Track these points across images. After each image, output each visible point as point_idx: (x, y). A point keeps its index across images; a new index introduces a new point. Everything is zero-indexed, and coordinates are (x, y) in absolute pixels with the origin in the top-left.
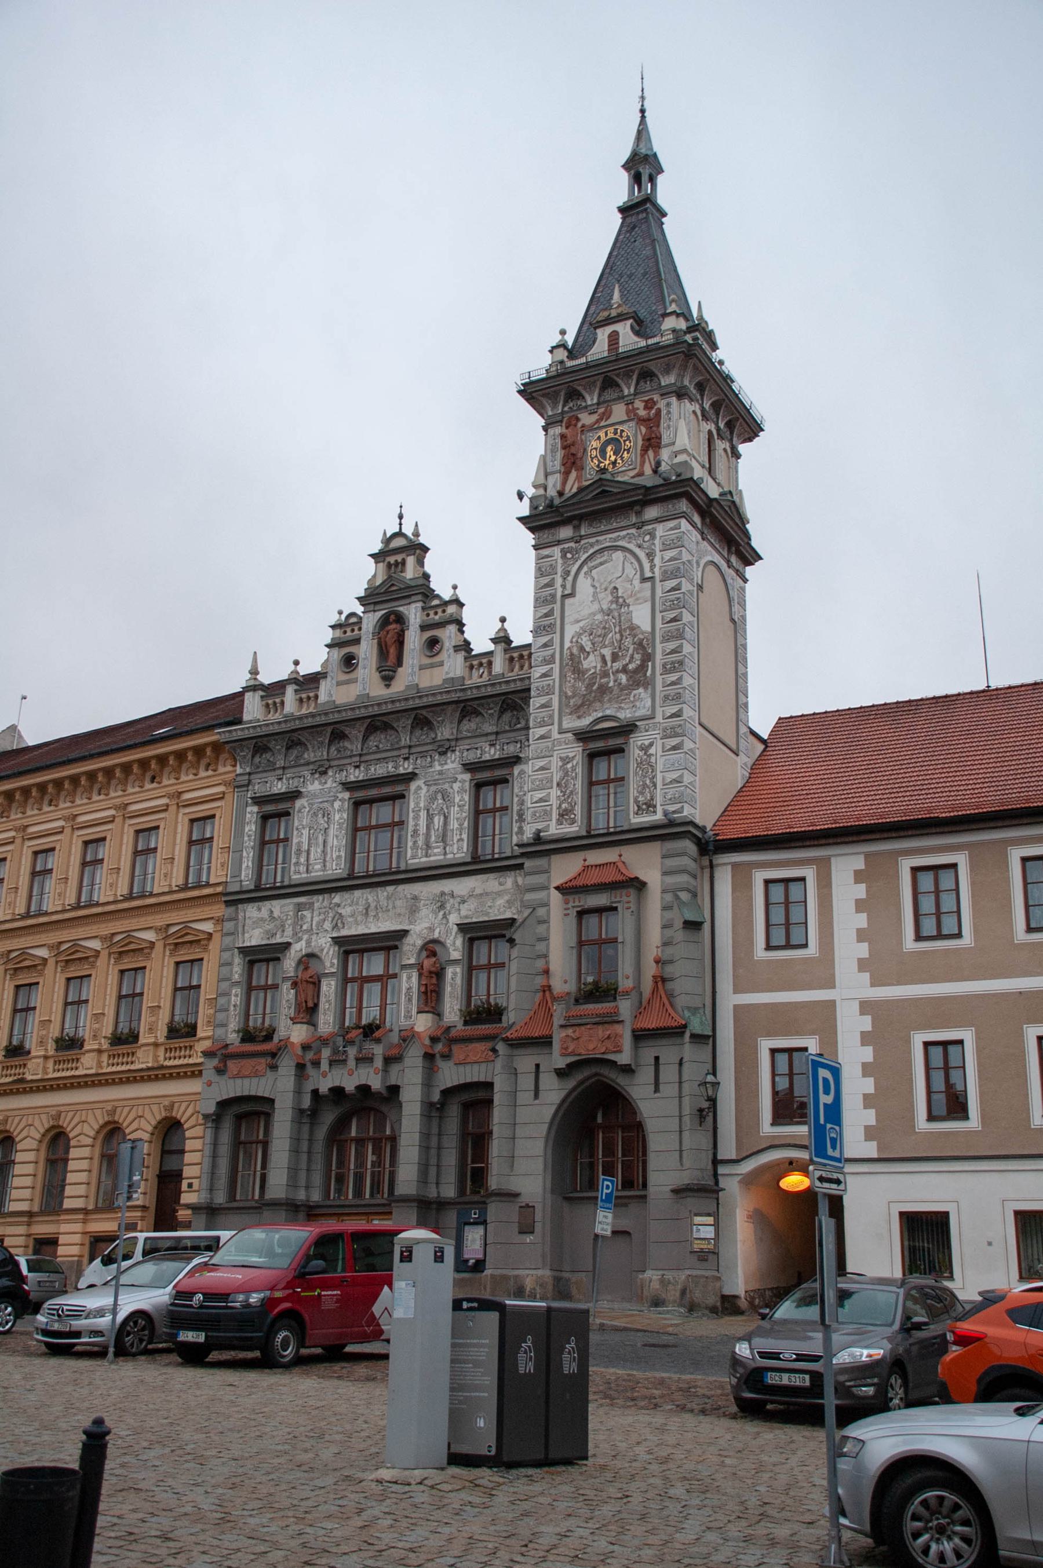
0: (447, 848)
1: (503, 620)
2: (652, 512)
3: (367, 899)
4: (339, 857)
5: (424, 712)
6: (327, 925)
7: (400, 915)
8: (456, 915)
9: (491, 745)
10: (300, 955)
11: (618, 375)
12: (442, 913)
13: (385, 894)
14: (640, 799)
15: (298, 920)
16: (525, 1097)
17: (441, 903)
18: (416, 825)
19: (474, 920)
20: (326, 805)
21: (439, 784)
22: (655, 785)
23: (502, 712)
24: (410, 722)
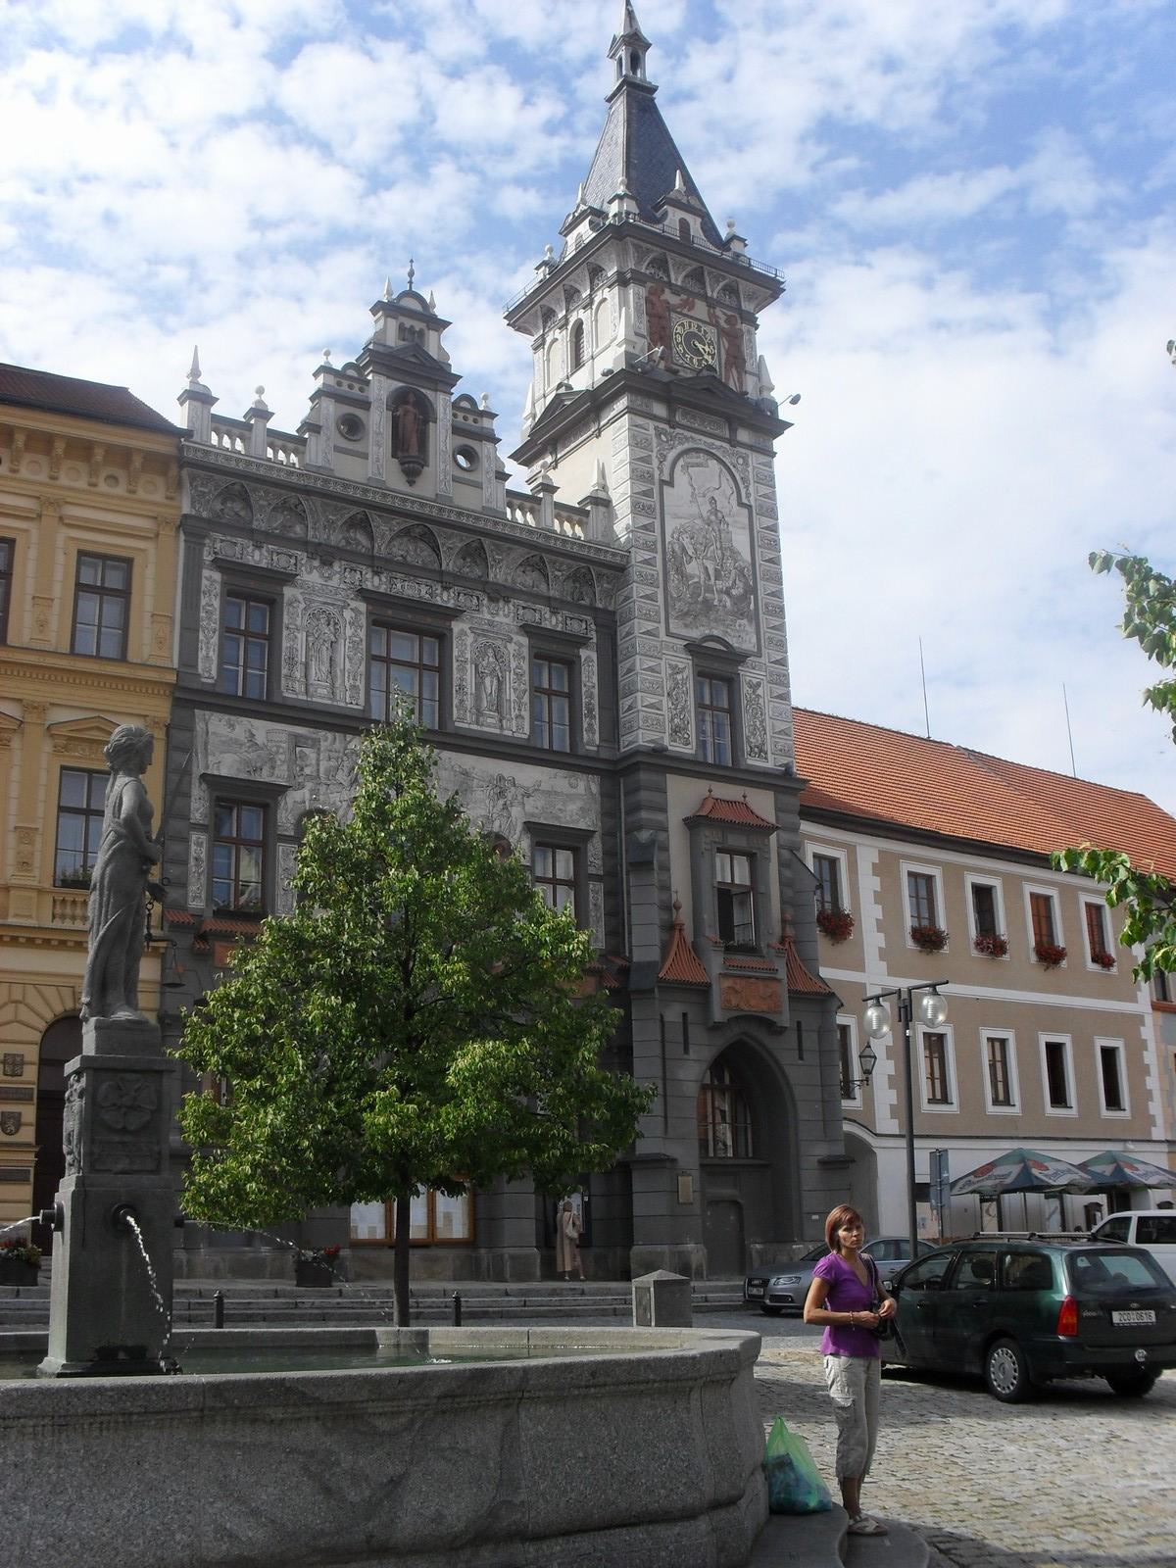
4: (354, 687)
5: (487, 543)
6: (341, 776)
10: (300, 809)
11: (710, 273)
12: (501, 802)
17: (500, 788)
24: (460, 545)
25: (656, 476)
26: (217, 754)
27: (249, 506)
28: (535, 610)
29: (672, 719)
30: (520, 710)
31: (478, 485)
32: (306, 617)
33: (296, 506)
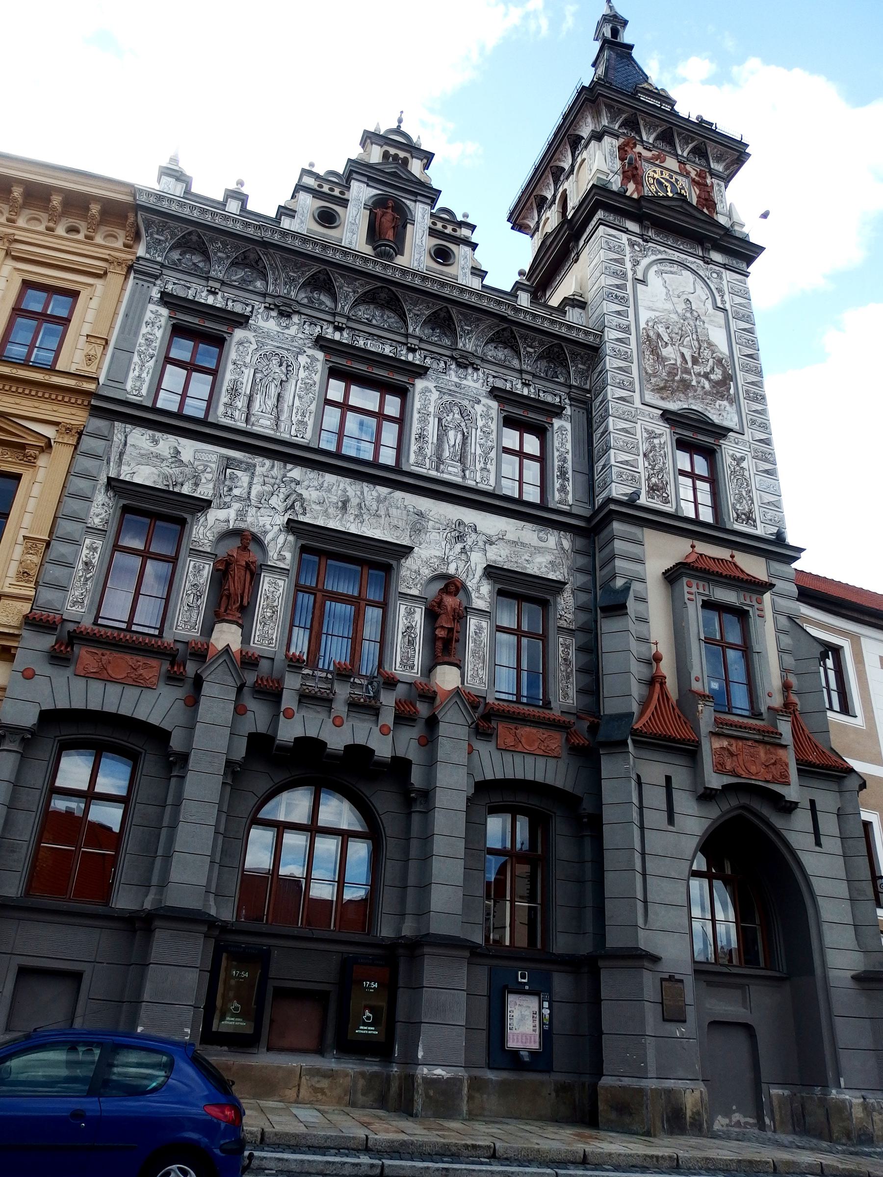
0: (467, 472)
2: (716, 256)
3: (345, 491)
8: (480, 554)
10: (223, 527)
11: (679, 134)
12: (459, 546)
13: (375, 494)
14: (738, 507)
16: (656, 818)
17: (459, 533)
20: (285, 353)
21: (456, 397)
22: (752, 500)
25: (630, 274)
26: (133, 465)
27: (207, 258)
28: (506, 380)
29: (649, 479)
33: (257, 262)
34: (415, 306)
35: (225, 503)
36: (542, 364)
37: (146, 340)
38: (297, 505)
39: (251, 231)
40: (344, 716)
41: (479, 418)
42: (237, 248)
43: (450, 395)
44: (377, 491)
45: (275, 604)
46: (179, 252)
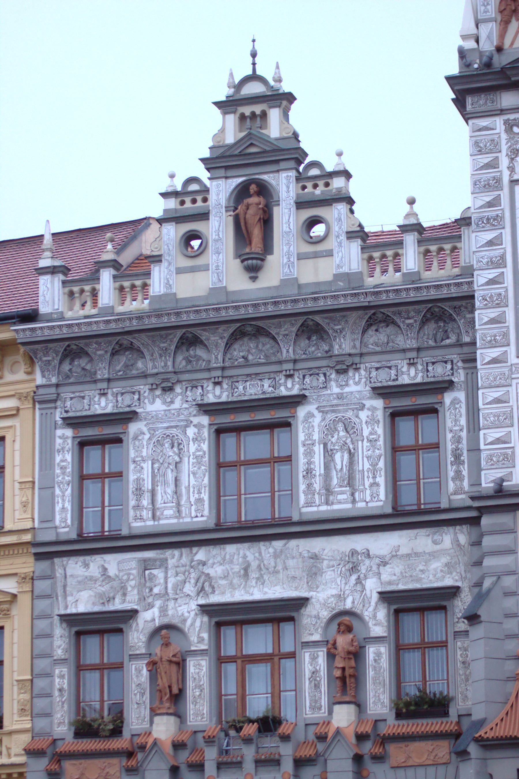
0: (357, 495)
1: (412, 202)
3: (245, 557)
4: (200, 501)
5: (317, 318)
6: (189, 588)
7: (294, 578)
9: (410, 364)
10: (151, 627)
12: (354, 577)
13: (271, 550)
15: (145, 581)
17: (352, 564)
18: (309, 463)
19: (401, 587)
20: (174, 431)
21: (339, 411)
23: (424, 322)
24: (294, 329)
26: (75, 593)
27: (91, 360)
28: (390, 368)
30: (374, 477)
31: (330, 254)
32: (151, 446)
34: (280, 327)
35: (149, 604)
36: (430, 328)
37: (61, 468)
38: (207, 584)
39: (113, 325)
40: (253, 772)
41: (364, 426)
42: (110, 342)
43: (333, 411)
44: (273, 547)
45: (201, 683)
46: (68, 361)
